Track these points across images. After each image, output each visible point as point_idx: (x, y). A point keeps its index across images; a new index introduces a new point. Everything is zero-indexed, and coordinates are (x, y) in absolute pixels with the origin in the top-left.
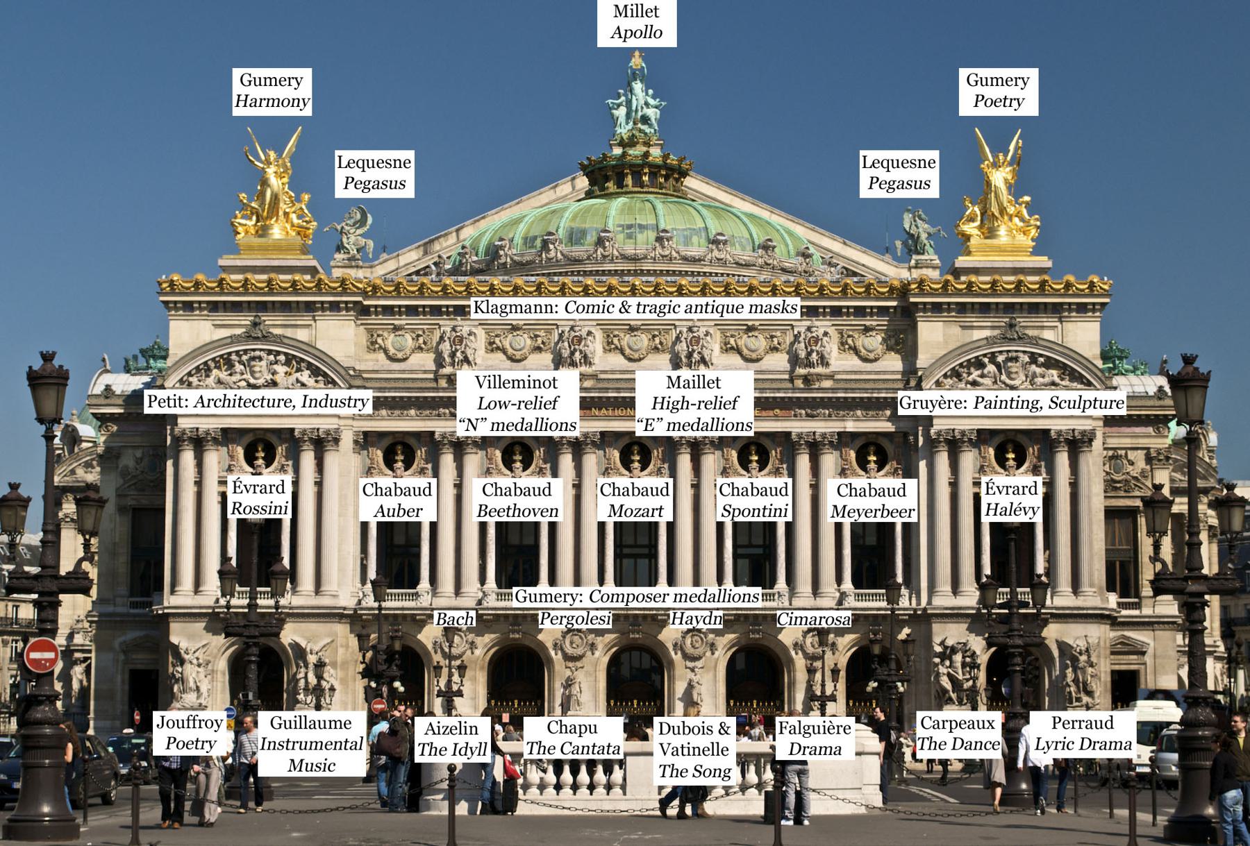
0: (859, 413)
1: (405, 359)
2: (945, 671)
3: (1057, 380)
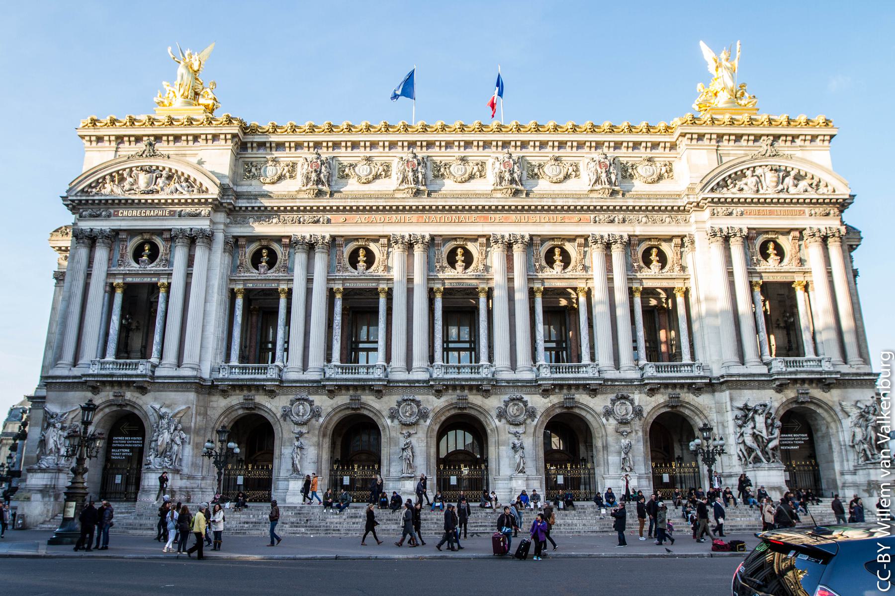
2: (751, 432)
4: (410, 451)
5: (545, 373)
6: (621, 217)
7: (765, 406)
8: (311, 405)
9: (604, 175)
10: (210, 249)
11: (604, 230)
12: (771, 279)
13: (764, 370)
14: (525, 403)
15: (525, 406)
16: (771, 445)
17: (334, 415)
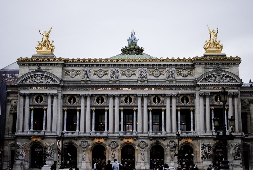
0: (182, 89)
1: (74, 77)
2: (204, 151)
3: (229, 81)
4: (114, 155)
5: (151, 135)
7: (209, 144)
8: (87, 143)
9: (171, 75)
10: (57, 98)
13: (211, 134)
14: (145, 142)
16: (209, 155)
17: (94, 145)
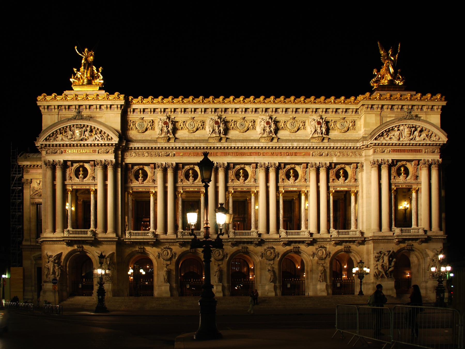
6: (326, 153)
8: (171, 251)
11: (317, 160)
12: (400, 186)
15: (274, 251)
